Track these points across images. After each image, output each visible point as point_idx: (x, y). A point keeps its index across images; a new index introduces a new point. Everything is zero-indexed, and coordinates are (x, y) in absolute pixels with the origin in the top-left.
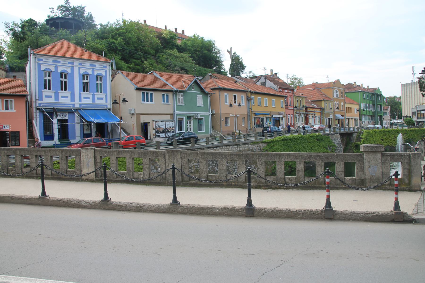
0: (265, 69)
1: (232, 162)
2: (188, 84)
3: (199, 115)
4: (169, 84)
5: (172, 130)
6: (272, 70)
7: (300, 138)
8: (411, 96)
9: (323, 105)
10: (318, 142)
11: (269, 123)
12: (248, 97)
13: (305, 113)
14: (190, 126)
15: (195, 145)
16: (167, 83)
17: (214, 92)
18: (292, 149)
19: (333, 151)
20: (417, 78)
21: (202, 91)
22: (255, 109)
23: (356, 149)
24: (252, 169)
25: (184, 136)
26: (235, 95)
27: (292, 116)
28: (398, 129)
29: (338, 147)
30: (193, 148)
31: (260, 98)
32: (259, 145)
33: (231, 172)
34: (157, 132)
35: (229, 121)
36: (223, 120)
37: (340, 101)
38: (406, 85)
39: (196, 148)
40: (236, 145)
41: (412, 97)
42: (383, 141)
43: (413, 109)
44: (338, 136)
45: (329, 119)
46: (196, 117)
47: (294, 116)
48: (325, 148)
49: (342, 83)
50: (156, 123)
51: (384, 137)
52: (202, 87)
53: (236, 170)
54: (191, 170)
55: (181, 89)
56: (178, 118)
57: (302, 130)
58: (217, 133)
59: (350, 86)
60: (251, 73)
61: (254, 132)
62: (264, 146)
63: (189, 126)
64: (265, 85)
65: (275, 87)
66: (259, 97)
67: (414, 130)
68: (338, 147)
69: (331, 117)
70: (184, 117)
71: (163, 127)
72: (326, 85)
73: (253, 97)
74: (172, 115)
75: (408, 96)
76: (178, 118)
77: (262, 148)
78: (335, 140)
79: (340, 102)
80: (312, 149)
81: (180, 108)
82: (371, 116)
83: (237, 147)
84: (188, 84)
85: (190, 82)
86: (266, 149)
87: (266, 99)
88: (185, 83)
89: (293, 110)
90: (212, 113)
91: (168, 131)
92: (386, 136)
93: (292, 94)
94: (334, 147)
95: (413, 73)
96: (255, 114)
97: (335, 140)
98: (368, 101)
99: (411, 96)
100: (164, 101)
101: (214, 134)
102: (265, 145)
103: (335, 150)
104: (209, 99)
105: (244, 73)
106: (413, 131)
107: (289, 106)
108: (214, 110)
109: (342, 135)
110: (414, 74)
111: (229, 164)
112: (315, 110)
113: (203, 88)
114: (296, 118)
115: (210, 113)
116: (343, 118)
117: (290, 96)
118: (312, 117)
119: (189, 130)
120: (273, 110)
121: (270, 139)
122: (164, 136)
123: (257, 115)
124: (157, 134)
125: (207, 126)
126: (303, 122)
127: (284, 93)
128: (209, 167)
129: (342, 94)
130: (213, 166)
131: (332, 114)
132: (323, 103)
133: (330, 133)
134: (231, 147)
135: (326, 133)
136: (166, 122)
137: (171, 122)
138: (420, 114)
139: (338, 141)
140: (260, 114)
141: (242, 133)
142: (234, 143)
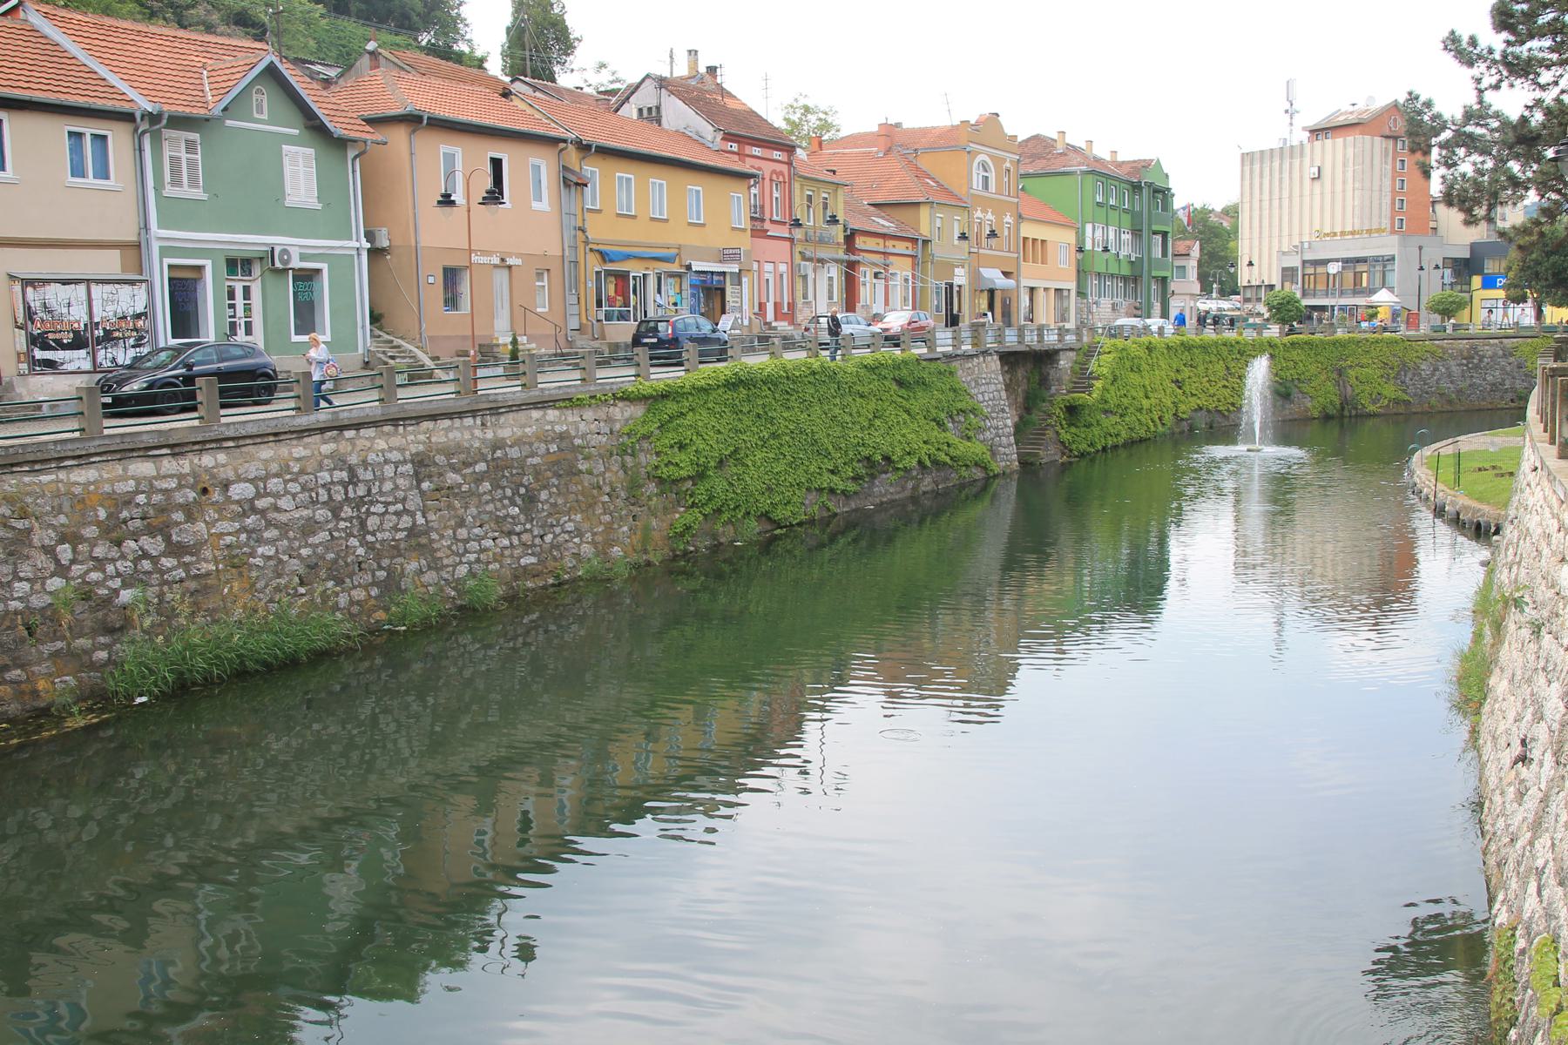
0: (671, 57)
1: (450, 507)
2: (230, 83)
3: (295, 254)
4: (113, 79)
5: (136, 330)
6: (696, 51)
7: (814, 373)
8: (1276, 203)
9: (926, 223)
10: (903, 392)
11: (672, 300)
12: (565, 168)
13: (846, 257)
14: (248, 308)
15: (224, 420)
16: (103, 72)
17: (379, 137)
18: (773, 429)
19: (971, 434)
20: (1304, 129)
21: (316, 128)
22: (598, 231)
23: (1070, 425)
24: (566, 537)
25: (193, 365)
26: (497, 155)
27: (783, 268)
28: (1240, 338)
29: (994, 415)
30: (208, 436)
31: (628, 180)
32: (602, 413)
33: (446, 562)
34: (39, 341)
35: (465, 288)
36: (431, 280)
37: (999, 208)
38: (1257, 156)
39: (231, 433)
40: (473, 413)
41: (1280, 207)
42: (1180, 388)
43: (1284, 257)
44: (994, 363)
45: (951, 286)
46: (278, 265)
47: (793, 269)
48: (934, 420)
49: (1009, 131)
50: (29, 290)
51: (1186, 372)
52: (314, 107)
53: (473, 545)
54: (198, 561)
55: (181, 109)
56: (171, 267)
57: (825, 337)
58: (399, 347)
59: (1038, 147)
60: (603, 70)
61: (596, 344)
62: (631, 418)
63: (240, 311)
64: (659, 122)
65: (707, 130)
66: (625, 173)
67: (1306, 343)
68: (994, 415)
69: (957, 281)
70: (208, 264)
71: (79, 315)
72: (940, 136)
73: (592, 169)
74: (135, 250)
75: (1266, 204)
76: (171, 267)
77: (617, 426)
78: (977, 384)
79: (999, 215)
80: (871, 425)
81: (175, 213)
82: (1125, 279)
83: (479, 422)
84: (230, 83)
85: (238, 76)
86: (643, 431)
87: (661, 185)
88: (212, 80)
89: (788, 244)
90: (369, 245)
91: (109, 338)
92: (1191, 366)
93: (784, 168)
94: (976, 416)
95: (1288, 106)
96: (604, 257)
97: (977, 384)
98: (1114, 215)
99: (1276, 203)
100: (78, 171)
101: (384, 352)
102: (638, 411)
103: (981, 430)
104: (354, 171)
105: (572, 71)
106: (1303, 348)
107: (772, 222)
108: (384, 231)
109: (1010, 359)
110: (1290, 113)
111: (431, 517)
112: (890, 243)
113: (319, 113)
114: (805, 277)
115: (357, 245)
116: (1011, 283)
117: (774, 177)
118: (876, 275)
119: (241, 331)
120: (691, 238)
121: (664, 377)
122: (87, 366)
123: (611, 261)
124: (39, 354)
125: (343, 312)
126: (835, 299)
127: (747, 159)
128: (310, 540)
129: (1006, 179)
130: (338, 530)
131: (963, 267)
132: (924, 212)
133: (959, 352)
134: (447, 423)
135: (939, 349)
136: (96, 290)
137: (127, 288)
138: (1312, 277)
139: (992, 387)
140: (628, 257)
141: (534, 345)
142: (463, 404)
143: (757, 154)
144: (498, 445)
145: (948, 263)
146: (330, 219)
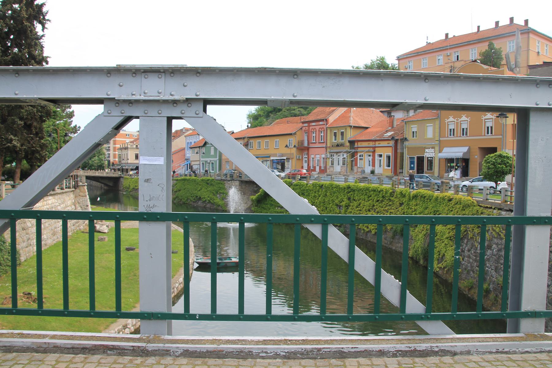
74: (199, 161)
107: (319, 143)
112: (377, 143)
145: (422, 147)
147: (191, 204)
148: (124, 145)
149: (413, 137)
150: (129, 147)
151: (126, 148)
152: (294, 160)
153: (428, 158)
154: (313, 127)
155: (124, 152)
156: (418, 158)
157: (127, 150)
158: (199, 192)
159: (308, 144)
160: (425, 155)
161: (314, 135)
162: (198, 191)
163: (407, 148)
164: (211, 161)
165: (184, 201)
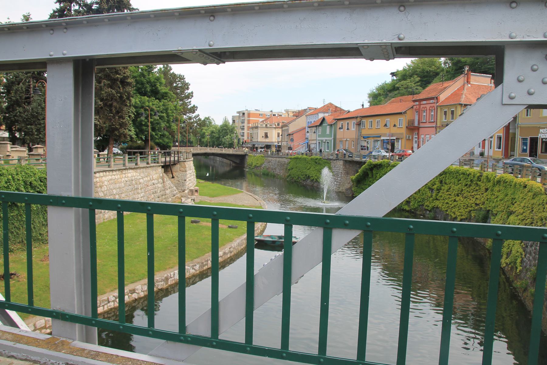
29: (336, 176)
107: (429, 122)
143: (432, 102)
144: (282, 161)
145: (536, 127)
146: (330, 136)
147: (301, 183)
148: (255, 124)
149: (527, 115)
150: (259, 126)
151: (257, 128)
152: (404, 140)
153: (542, 139)
154: (424, 106)
155: (255, 131)
156: (532, 139)
157: (257, 129)
158: (308, 171)
159: (419, 123)
160: (539, 136)
161: (425, 114)
162: (307, 169)
163: (519, 128)
164: (326, 140)
165: (295, 179)
